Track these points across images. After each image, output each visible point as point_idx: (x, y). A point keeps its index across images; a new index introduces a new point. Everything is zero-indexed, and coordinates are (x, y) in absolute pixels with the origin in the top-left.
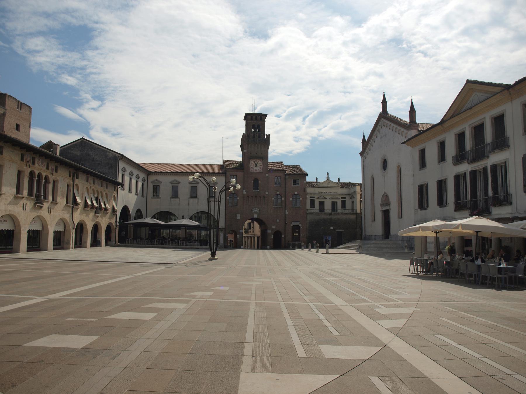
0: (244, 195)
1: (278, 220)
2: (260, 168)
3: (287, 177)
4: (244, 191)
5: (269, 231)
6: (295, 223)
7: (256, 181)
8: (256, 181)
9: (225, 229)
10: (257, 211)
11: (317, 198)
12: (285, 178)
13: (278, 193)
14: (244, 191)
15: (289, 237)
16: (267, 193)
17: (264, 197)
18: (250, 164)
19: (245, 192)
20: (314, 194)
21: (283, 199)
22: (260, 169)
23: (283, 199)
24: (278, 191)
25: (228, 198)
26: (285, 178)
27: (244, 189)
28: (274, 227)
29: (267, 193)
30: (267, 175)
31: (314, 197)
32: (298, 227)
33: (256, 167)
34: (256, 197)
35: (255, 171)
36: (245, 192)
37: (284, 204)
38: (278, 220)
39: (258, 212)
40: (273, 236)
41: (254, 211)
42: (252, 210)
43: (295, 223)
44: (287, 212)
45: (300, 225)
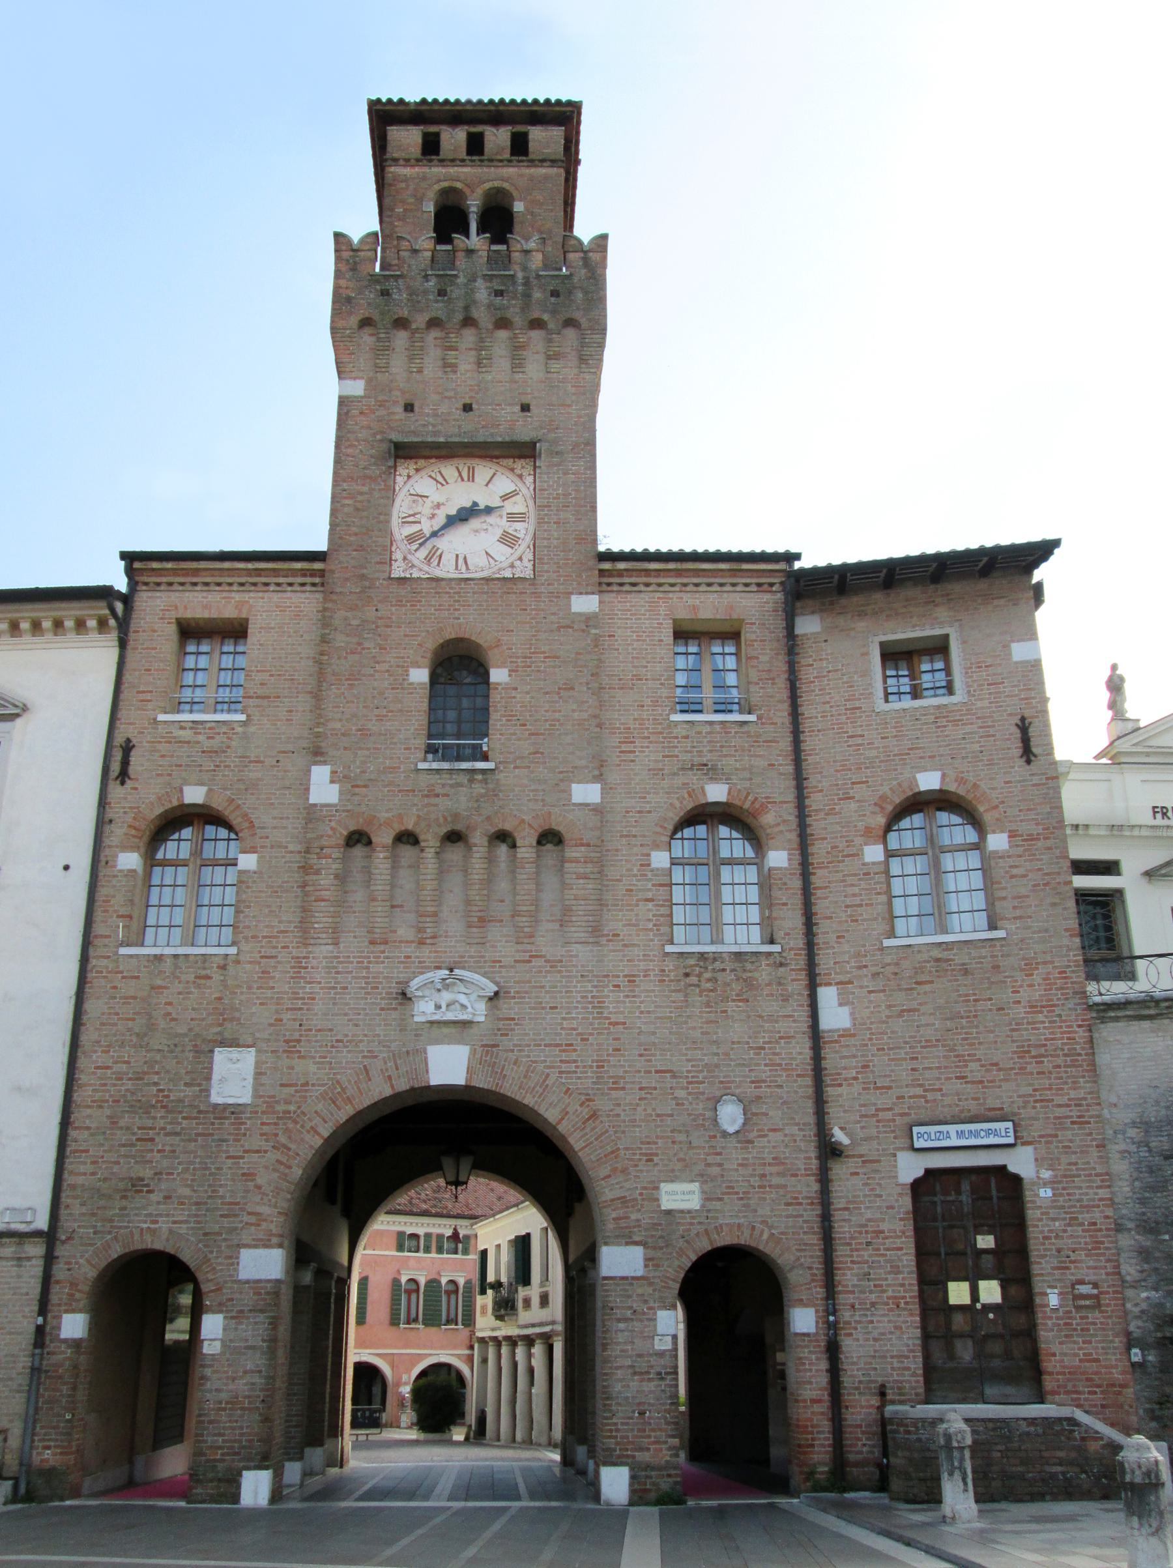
0: (312, 814)
1: (730, 1116)
2: (508, 539)
3: (808, 625)
4: (320, 774)
5: (618, 1261)
6: (952, 1135)
7: (459, 667)
8: (459, 667)
9: (50, 1237)
10: (469, 1001)
11: (1149, 874)
12: (791, 643)
13: (716, 793)
14: (320, 774)
15: (884, 1341)
16: (586, 793)
17: (550, 838)
18: (401, 506)
19: (323, 788)
20: (1116, 830)
21: (778, 858)
22: (503, 554)
23: (778, 858)
24: (711, 772)
25: (130, 860)
26: (791, 643)
27: (317, 754)
28: (680, 1196)
29: (586, 793)
30: (585, 604)
31: (1109, 868)
32: (998, 1193)
33: (465, 531)
34: (454, 837)
35: (447, 570)
36: (323, 788)
37: (791, 921)
38: (730, 1116)
39: (478, 1011)
40: (671, 1324)
41: (424, 1009)
42: (405, 997)
43: (958, 1144)
44: (835, 1015)
45: (1021, 1163)
